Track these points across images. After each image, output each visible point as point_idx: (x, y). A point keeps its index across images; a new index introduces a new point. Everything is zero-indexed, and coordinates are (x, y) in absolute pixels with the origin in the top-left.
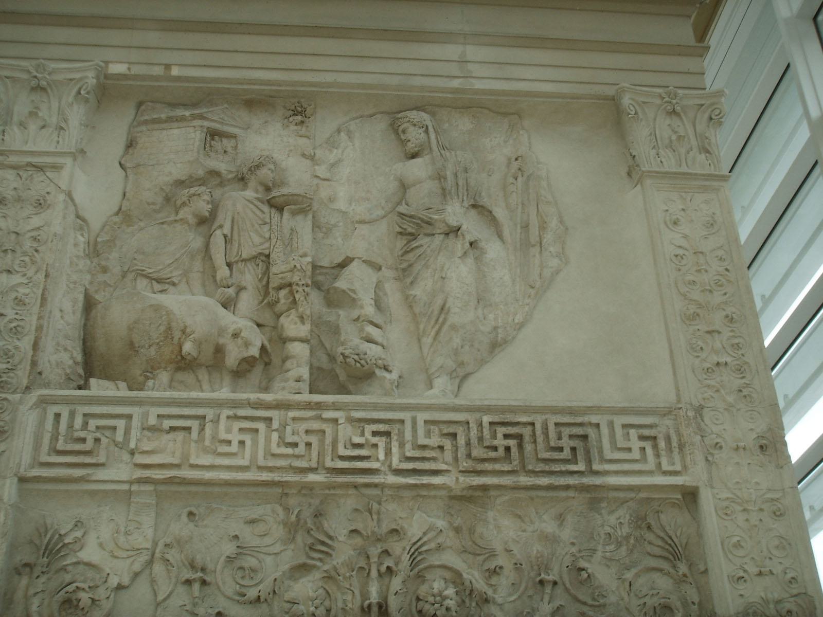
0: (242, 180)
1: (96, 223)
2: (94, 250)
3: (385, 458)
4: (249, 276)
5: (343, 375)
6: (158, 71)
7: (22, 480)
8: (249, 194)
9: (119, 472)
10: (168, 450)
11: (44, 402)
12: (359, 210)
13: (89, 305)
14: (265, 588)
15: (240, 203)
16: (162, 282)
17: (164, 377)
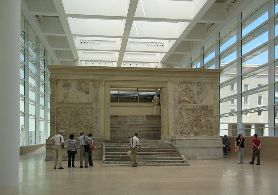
0: (188, 89)
1: (179, 92)
2: (180, 94)
3: (197, 108)
4: (189, 96)
5: (194, 103)
6: (183, 81)
7: (179, 109)
8: (189, 90)
9: (184, 109)
10: (186, 108)
11: (179, 105)
12: (195, 91)
13: (180, 98)
14: (191, 114)
15: (188, 90)
16: (184, 96)
17: (184, 102)
